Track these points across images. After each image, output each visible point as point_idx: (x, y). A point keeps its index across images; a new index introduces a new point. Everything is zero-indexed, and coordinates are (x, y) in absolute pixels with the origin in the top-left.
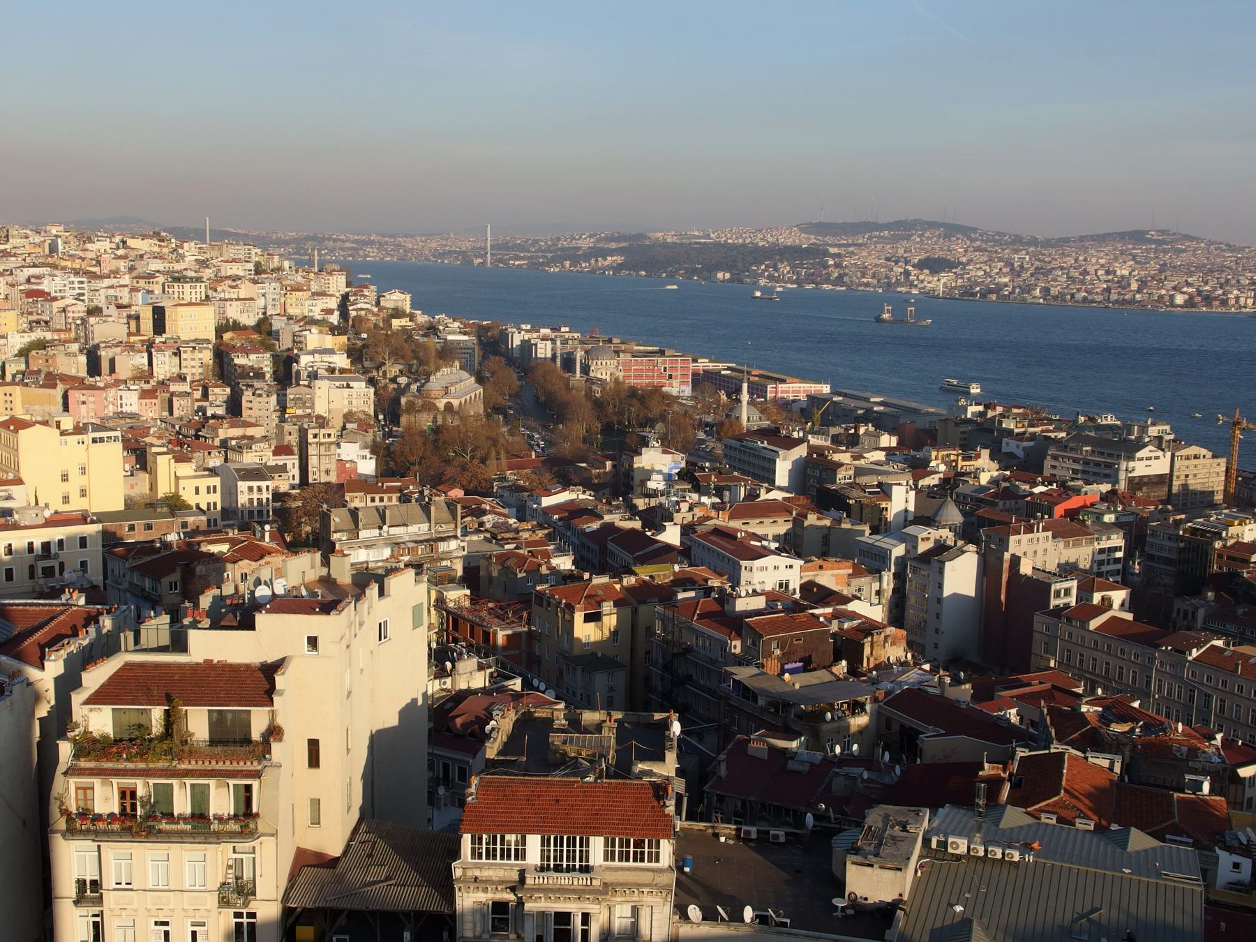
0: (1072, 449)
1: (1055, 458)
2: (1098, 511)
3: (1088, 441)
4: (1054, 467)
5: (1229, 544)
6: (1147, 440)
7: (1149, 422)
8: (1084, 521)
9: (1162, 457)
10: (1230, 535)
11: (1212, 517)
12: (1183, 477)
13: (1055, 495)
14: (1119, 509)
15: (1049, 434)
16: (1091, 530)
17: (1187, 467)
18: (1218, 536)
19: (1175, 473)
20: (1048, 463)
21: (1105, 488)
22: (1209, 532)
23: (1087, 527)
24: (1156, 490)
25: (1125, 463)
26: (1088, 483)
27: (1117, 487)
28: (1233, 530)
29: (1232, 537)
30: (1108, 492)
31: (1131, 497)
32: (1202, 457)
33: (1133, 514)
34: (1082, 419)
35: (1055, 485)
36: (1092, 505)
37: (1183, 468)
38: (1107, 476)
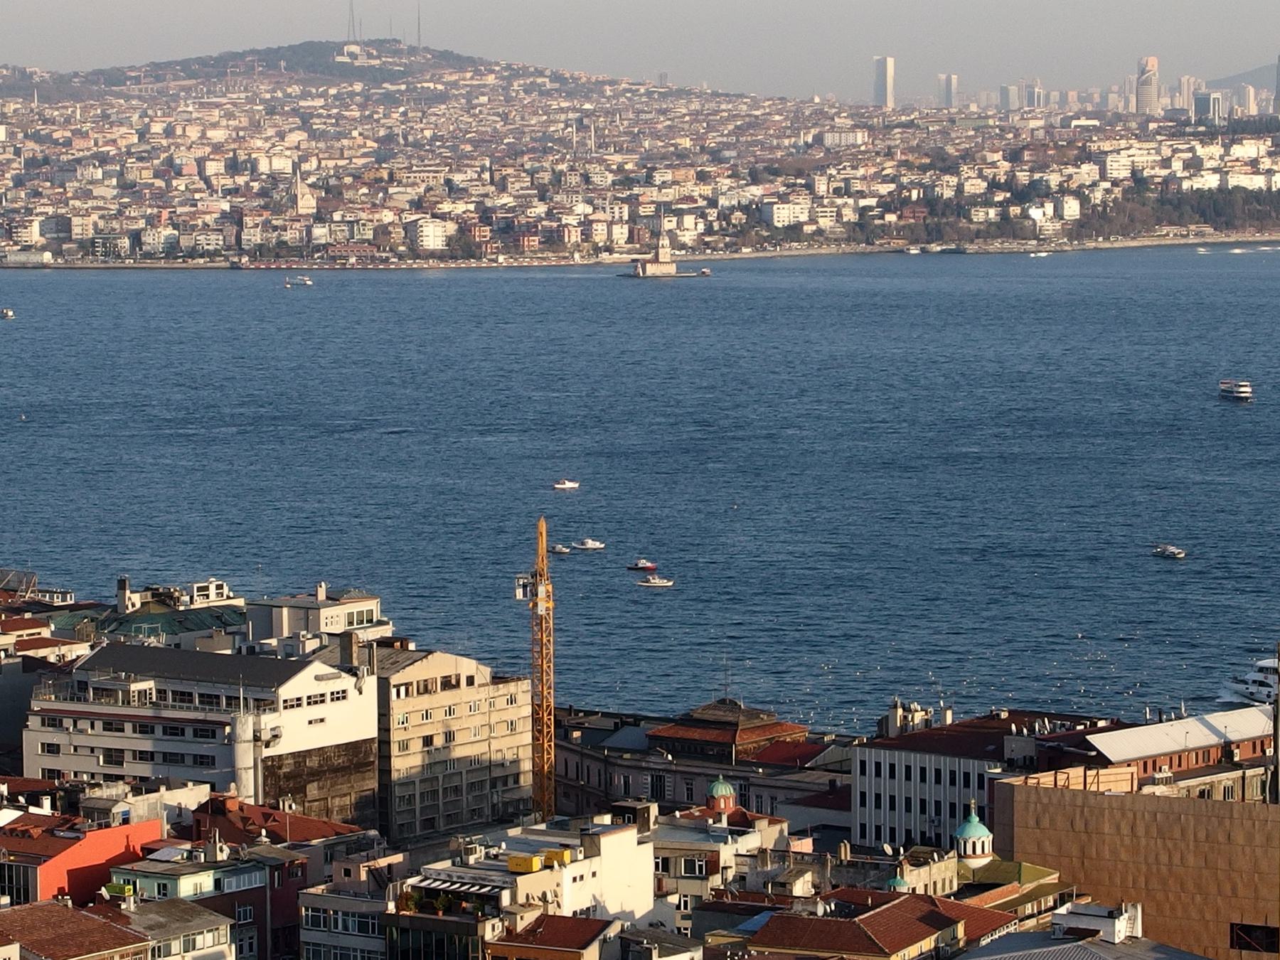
0: (102, 692)
1: (52, 720)
2: (160, 868)
3: (143, 662)
4: (52, 749)
5: (521, 926)
6: (311, 645)
7: (322, 594)
8: (117, 899)
9: (352, 693)
10: (521, 899)
11: (470, 852)
12: (417, 746)
13: (36, 832)
14: (222, 856)
15: (41, 653)
16: (136, 927)
17: (427, 715)
18: (490, 904)
19: (396, 736)
20: (34, 737)
21: (192, 796)
22: (467, 896)
23: (125, 919)
24: (344, 788)
25: (251, 719)
26: (142, 786)
27: (233, 792)
28: (528, 885)
29: (528, 905)
30: (202, 808)
31: (266, 817)
32: (463, 682)
33: (258, 864)
34: (135, 600)
35: (47, 802)
36: (148, 850)
37: (416, 719)
38: (203, 761)
